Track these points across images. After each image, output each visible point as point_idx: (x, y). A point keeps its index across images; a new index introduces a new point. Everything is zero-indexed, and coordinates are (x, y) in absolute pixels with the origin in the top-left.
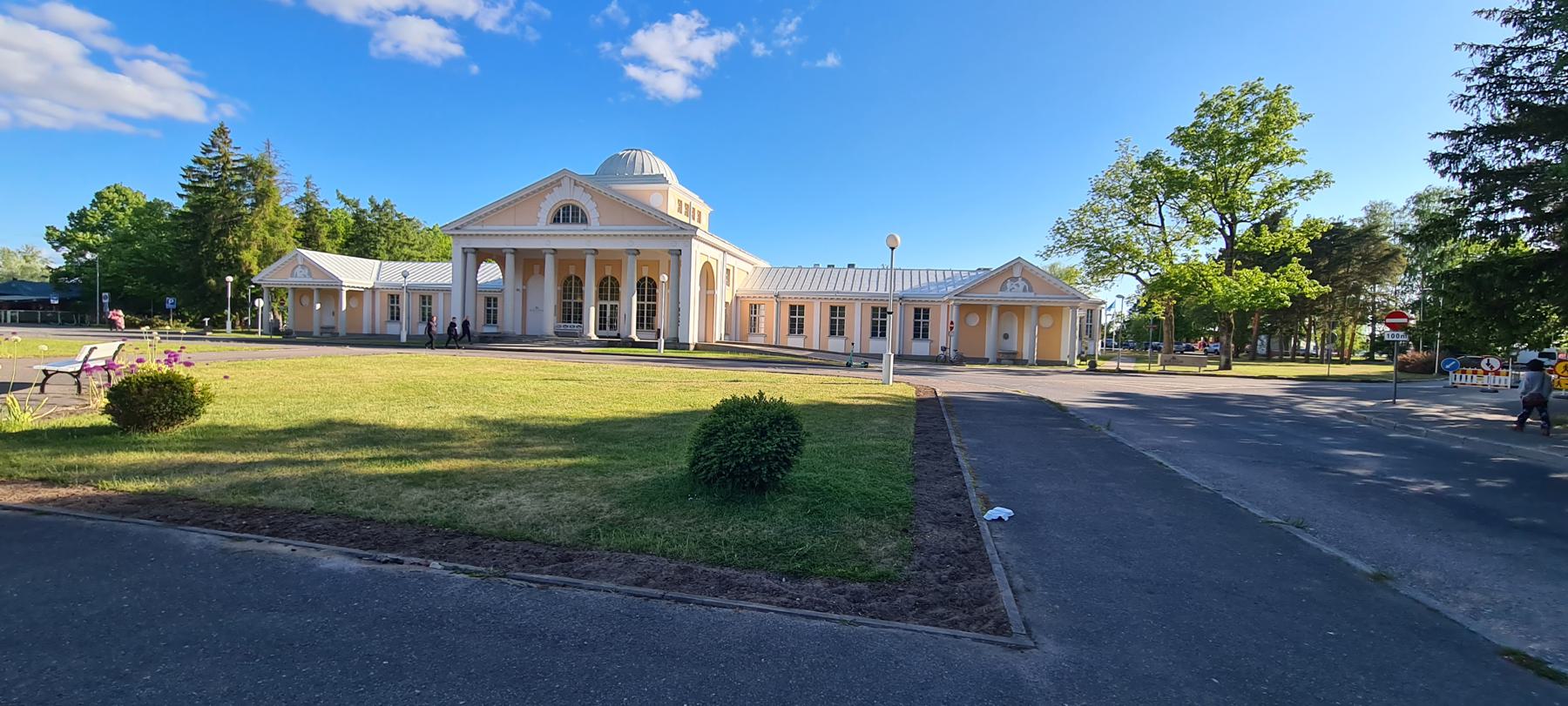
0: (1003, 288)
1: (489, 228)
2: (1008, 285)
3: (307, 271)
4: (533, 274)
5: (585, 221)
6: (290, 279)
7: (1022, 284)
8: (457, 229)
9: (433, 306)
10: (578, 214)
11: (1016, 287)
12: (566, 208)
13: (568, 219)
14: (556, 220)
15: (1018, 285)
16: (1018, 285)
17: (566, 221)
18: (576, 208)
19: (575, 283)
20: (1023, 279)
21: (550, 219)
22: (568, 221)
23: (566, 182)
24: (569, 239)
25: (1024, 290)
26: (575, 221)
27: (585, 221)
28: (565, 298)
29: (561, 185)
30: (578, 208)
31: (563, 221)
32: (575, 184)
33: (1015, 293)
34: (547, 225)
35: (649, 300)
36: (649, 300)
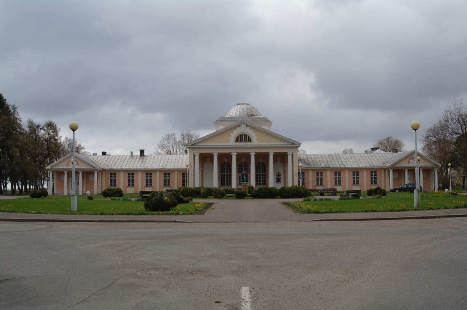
2: (411, 160)
5: (250, 140)
6: (67, 167)
8: (192, 145)
11: (414, 162)
12: (241, 136)
14: (237, 141)
15: (414, 161)
17: (241, 141)
18: (245, 136)
21: (235, 140)
22: (246, 141)
24: (244, 147)
26: (246, 141)
27: (250, 140)
29: (240, 126)
30: (247, 136)
31: (240, 141)
34: (234, 143)
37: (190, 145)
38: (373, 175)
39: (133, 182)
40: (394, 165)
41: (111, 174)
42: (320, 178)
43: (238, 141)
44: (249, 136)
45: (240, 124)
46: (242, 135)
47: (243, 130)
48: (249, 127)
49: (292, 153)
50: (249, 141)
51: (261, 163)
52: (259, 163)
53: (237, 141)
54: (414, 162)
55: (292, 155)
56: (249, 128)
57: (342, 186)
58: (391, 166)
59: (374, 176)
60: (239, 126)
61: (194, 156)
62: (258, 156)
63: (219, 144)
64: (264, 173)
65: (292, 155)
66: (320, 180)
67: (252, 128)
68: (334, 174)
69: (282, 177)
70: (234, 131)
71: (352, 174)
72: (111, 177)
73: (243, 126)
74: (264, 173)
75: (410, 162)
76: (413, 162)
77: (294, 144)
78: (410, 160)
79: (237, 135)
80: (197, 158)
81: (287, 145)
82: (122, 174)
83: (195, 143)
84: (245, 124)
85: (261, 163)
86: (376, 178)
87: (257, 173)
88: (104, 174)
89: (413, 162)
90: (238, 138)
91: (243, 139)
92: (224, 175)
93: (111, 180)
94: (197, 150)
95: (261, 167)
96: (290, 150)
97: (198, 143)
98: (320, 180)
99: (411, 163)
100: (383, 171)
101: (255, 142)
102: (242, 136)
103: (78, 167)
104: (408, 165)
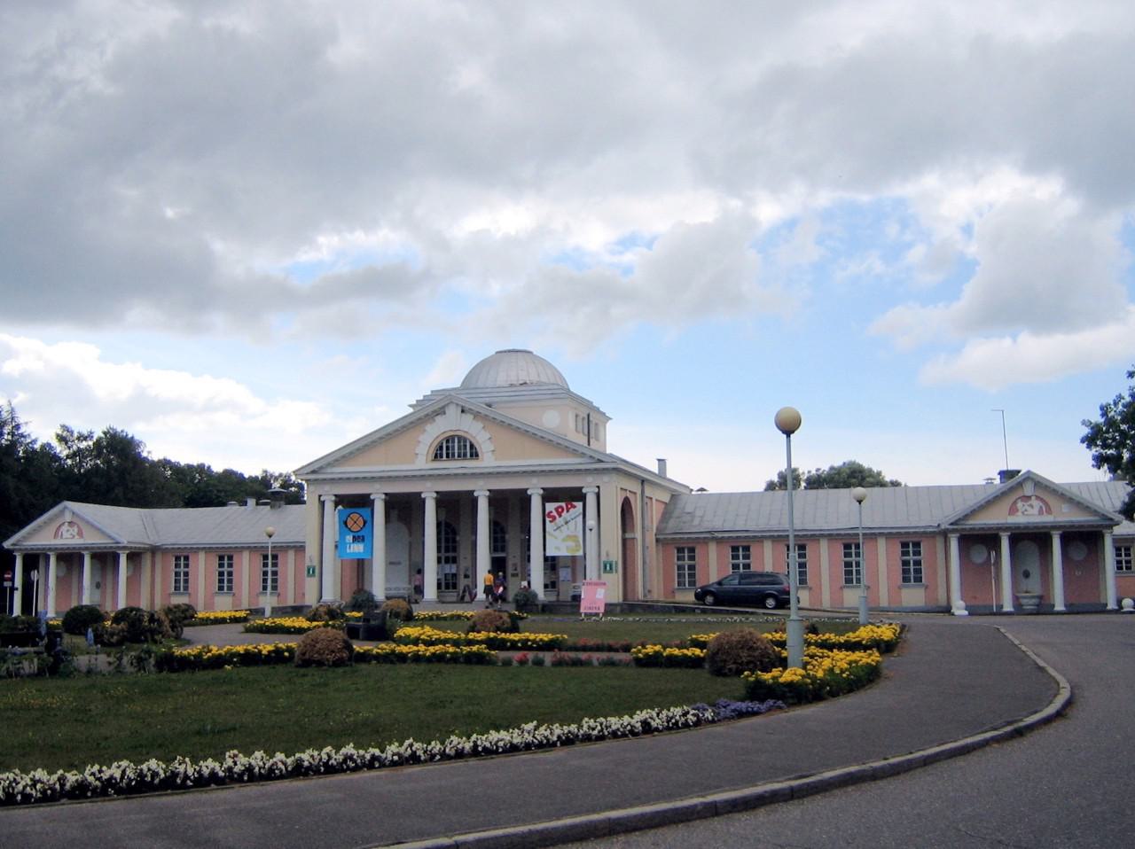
2: (1020, 504)
3: (76, 530)
5: (475, 454)
7: (1036, 503)
8: (313, 472)
10: (465, 446)
11: (1029, 508)
13: (453, 455)
14: (437, 457)
15: (1032, 506)
16: (1032, 506)
21: (431, 456)
24: (456, 475)
25: (1041, 512)
26: (462, 456)
27: (475, 454)
29: (445, 413)
30: (465, 440)
31: (448, 456)
32: (463, 411)
33: (1029, 515)
37: (307, 474)
39: (230, 581)
40: (960, 519)
42: (743, 565)
44: (473, 441)
45: (443, 407)
46: (453, 437)
47: (450, 423)
48: (472, 414)
49: (597, 490)
50: (471, 456)
53: (437, 457)
54: (1030, 511)
55: (598, 495)
56: (469, 417)
57: (810, 589)
58: (952, 524)
59: (911, 558)
60: (441, 411)
62: (499, 501)
63: (388, 468)
65: (598, 495)
66: (912, 567)
68: (899, 549)
70: (429, 427)
73: (453, 412)
75: (1017, 511)
76: (1026, 510)
77: (601, 461)
78: (1015, 503)
79: (439, 440)
81: (581, 464)
82: (712, 548)
84: (457, 405)
86: (918, 563)
89: (1026, 510)
91: (456, 451)
94: (327, 488)
96: (590, 479)
97: (329, 465)
98: (912, 567)
99: (1019, 513)
101: (487, 461)
102: (453, 442)
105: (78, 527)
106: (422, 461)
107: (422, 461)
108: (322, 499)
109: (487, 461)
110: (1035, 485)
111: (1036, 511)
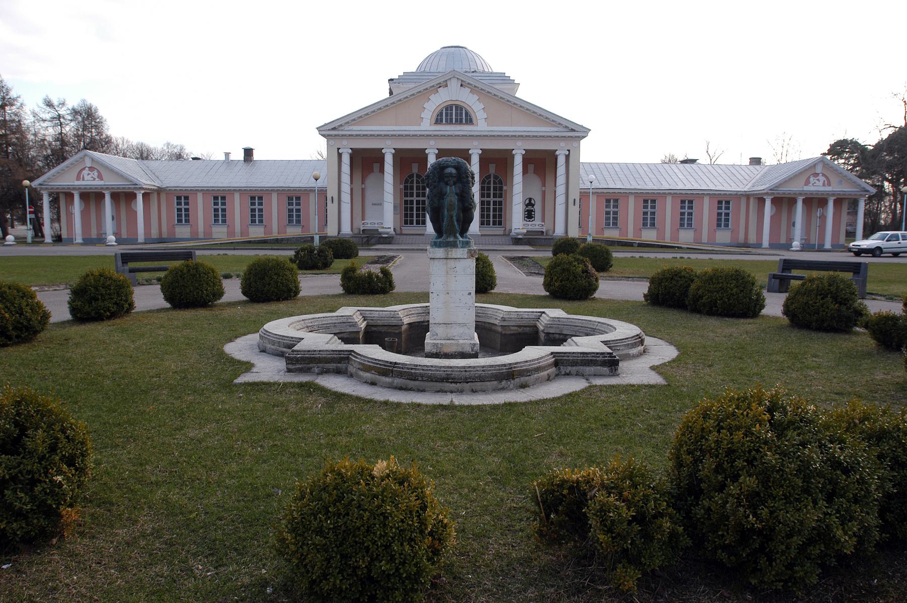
0: (807, 183)
1: (350, 128)
2: (812, 179)
4: (373, 172)
5: (469, 121)
7: (822, 179)
8: (334, 129)
9: (716, 211)
12: (449, 108)
13: (461, 119)
14: (438, 121)
15: (818, 180)
16: (818, 180)
17: (450, 122)
18: (459, 108)
19: (417, 181)
20: (824, 175)
21: (434, 121)
23: (454, 81)
25: (824, 185)
26: (459, 122)
27: (469, 121)
28: (406, 195)
29: (447, 86)
31: (446, 121)
32: (461, 85)
35: (418, 196)
36: (418, 196)
38: (721, 209)
40: (776, 187)
41: (179, 198)
43: (441, 121)
44: (468, 109)
49: (567, 153)
51: (492, 177)
52: (489, 177)
53: (438, 121)
55: (567, 157)
56: (467, 90)
61: (340, 155)
62: (487, 158)
64: (498, 199)
67: (474, 89)
69: (537, 208)
70: (432, 97)
71: (716, 205)
72: (179, 204)
73: (454, 85)
74: (498, 199)
75: (810, 183)
76: (815, 183)
77: (573, 130)
78: (809, 177)
79: (440, 108)
80: (346, 159)
83: (341, 125)
85: (492, 177)
87: (483, 199)
88: (163, 197)
89: (815, 183)
90: (441, 114)
91: (454, 117)
92: (412, 202)
93: (179, 210)
94: (345, 142)
95: (492, 186)
96: (563, 144)
100: (743, 201)
101: (481, 125)
102: (452, 110)
103: (102, 183)
104: (806, 188)
105: (98, 172)
106: (427, 125)
107: (427, 125)
108: (340, 151)
109: (481, 125)
110: (824, 166)
111: (821, 183)
